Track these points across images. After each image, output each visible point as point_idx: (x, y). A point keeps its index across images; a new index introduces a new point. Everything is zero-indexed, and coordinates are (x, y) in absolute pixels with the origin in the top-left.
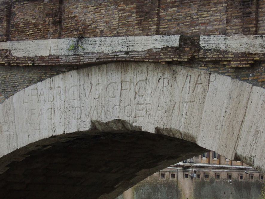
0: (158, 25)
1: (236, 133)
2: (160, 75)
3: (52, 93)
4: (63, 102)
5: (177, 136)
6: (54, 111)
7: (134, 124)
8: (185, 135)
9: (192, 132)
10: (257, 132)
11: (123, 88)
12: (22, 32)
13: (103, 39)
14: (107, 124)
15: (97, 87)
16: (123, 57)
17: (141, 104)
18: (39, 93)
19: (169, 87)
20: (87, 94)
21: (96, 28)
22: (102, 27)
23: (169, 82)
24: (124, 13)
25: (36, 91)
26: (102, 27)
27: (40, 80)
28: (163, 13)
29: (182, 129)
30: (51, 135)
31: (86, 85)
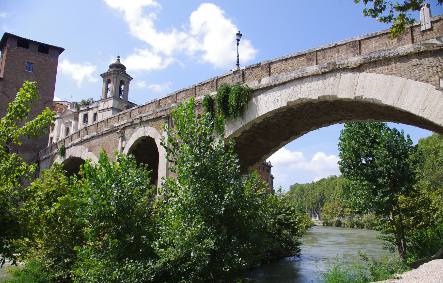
0: (317, 61)
1: (354, 89)
2: (318, 79)
5: (328, 98)
7: (308, 98)
8: (332, 96)
9: (335, 94)
10: (363, 87)
12: (250, 79)
14: (294, 101)
28: (318, 58)
29: (330, 94)
30: (267, 112)
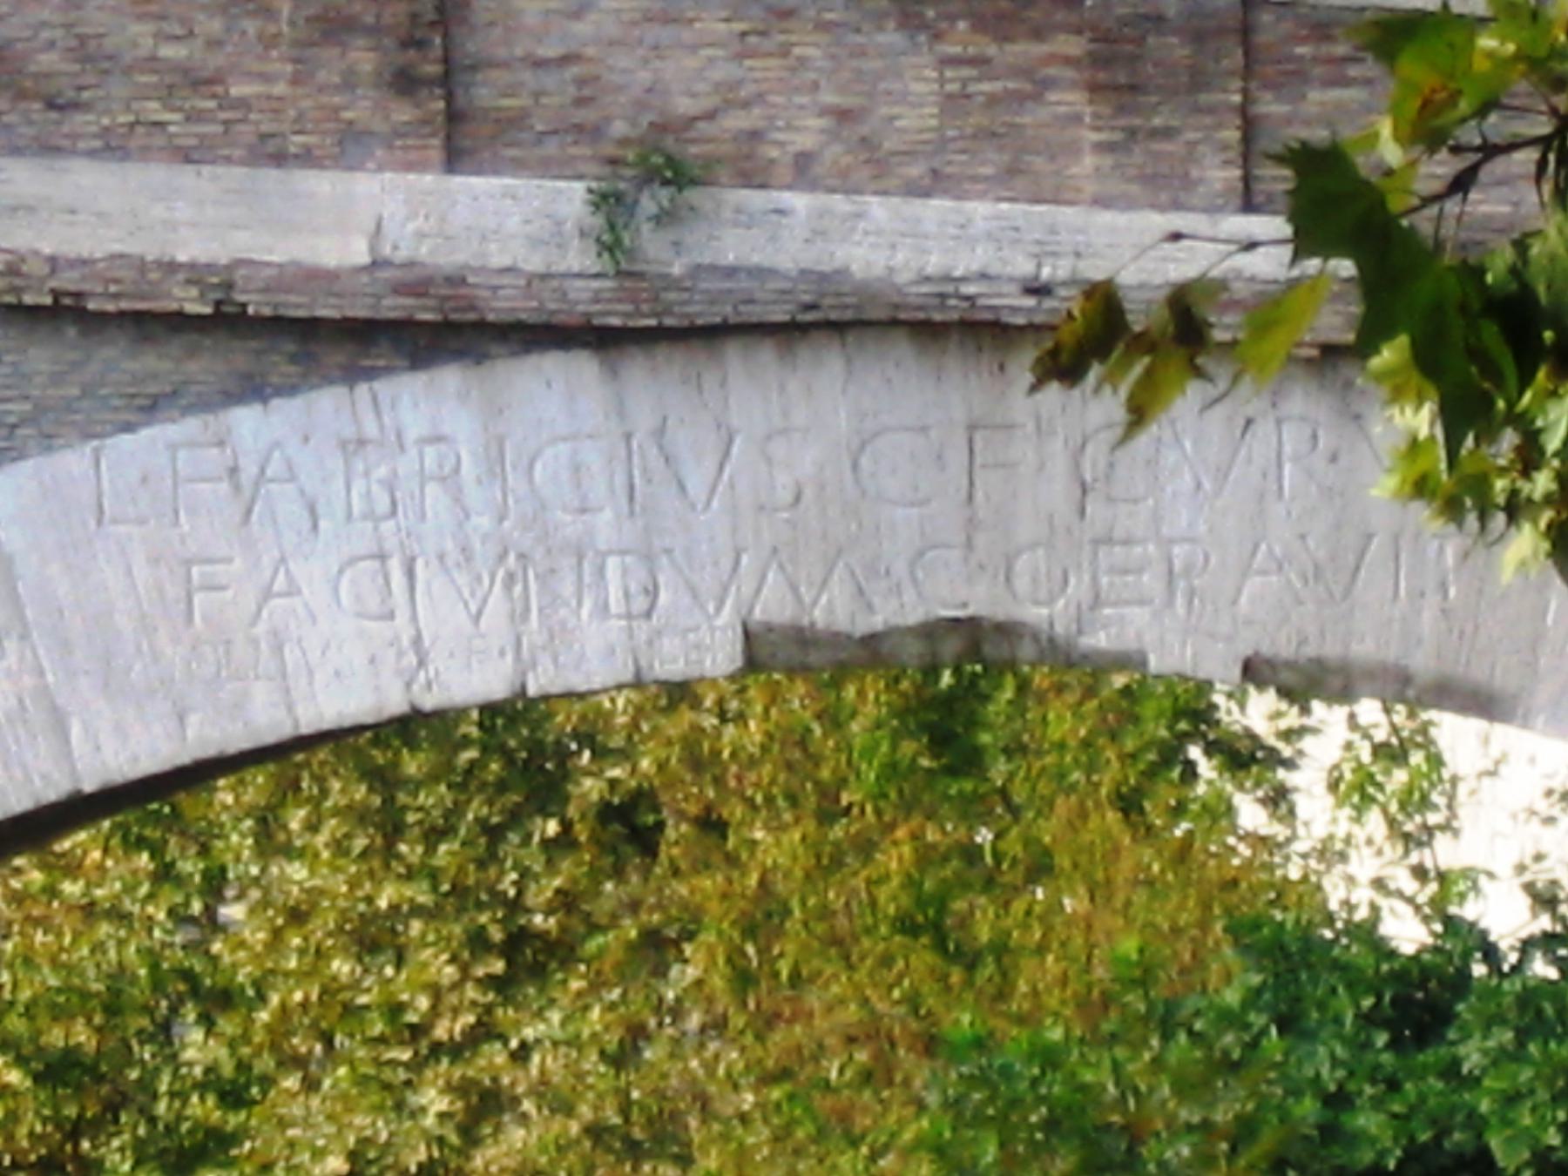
3: (382, 471)
4: (483, 522)
6: (410, 574)
11: (978, 460)
13: (839, 203)
15: (778, 448)
16: (1015, 310)
17: (1127, 542)
18: (249, 470)
19: (1319, 461)
20: (696, 484)
21: (755, 135)
22: (808, 133)
23: (1315, 437)
24: (979, 80)
25: (213, 458)
26: (808, 133)
27: (253, 389)
31: (680, 438)
